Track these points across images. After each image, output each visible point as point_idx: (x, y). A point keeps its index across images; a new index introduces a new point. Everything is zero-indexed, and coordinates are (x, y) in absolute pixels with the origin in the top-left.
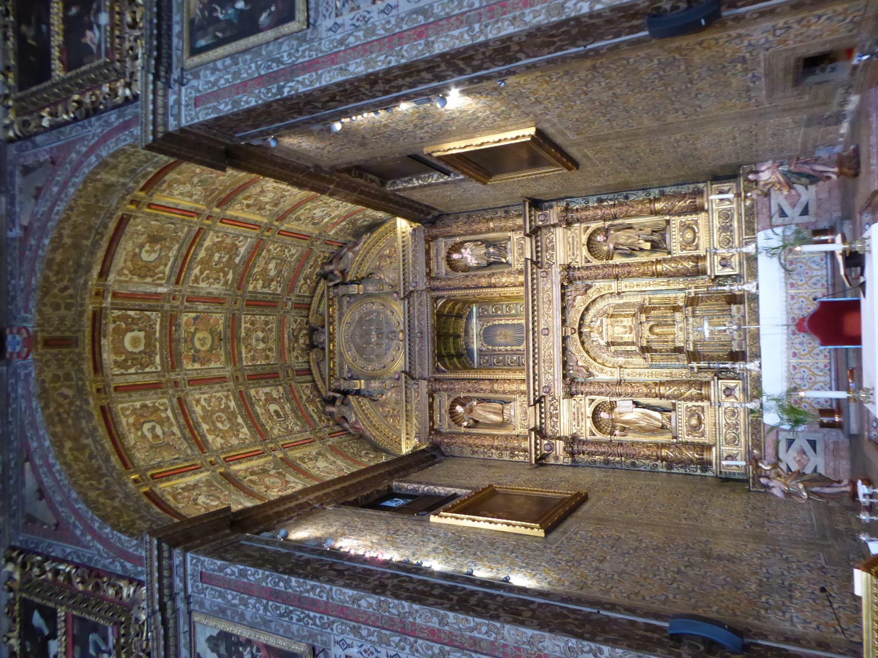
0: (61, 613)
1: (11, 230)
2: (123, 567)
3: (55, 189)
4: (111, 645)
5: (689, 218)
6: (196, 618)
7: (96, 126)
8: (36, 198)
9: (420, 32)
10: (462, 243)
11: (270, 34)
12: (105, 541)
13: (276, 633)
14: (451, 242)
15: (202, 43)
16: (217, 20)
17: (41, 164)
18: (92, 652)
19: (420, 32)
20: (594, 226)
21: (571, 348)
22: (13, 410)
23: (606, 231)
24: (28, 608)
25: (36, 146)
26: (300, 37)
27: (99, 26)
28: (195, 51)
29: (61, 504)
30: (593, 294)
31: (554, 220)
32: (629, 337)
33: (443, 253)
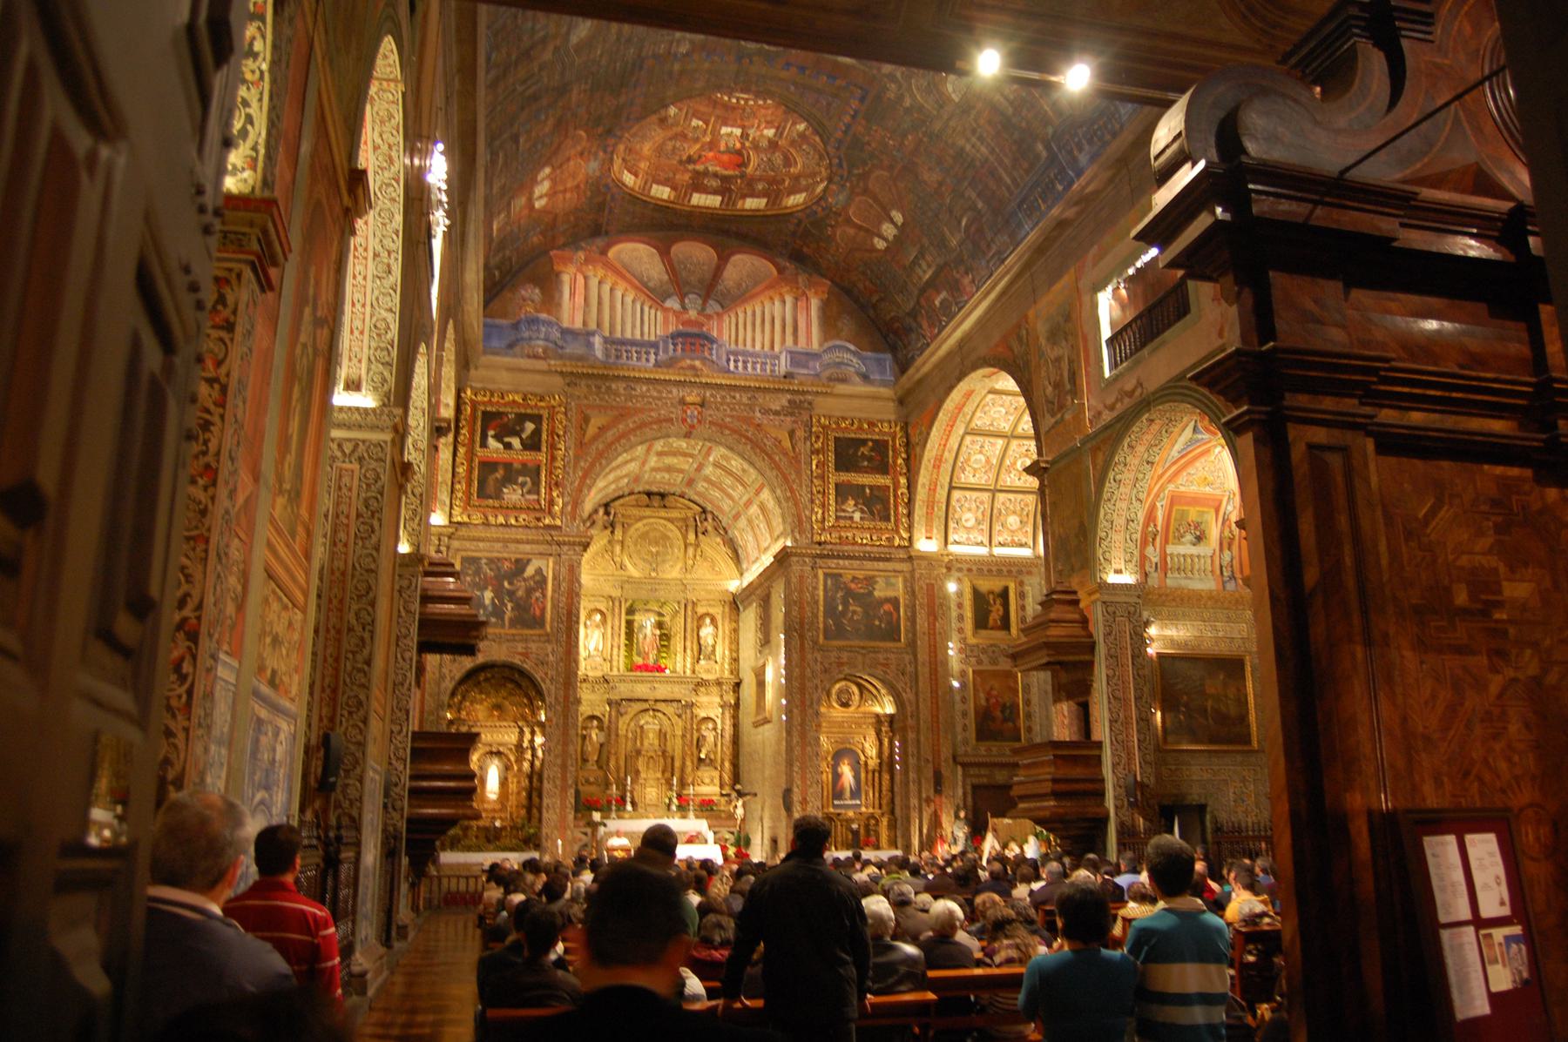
0: (542, 457)
4: (528, 497)
5: (717, 781)
6: (551, 560)
7: (805, 498)
9: (803, 702)
10: (716, 627)
11: (821, 626)
14: (719, 618)
15: (829, 582)
18: (521, 479)
19: (803, 702)
20: (719, 722)
21: (639, 704)
23: (715, 729)
24: (537, 419)
28: (826, 575)
30: (675, 719)
31: (725, 698)
32: (646, 743)
33: (711, 611)
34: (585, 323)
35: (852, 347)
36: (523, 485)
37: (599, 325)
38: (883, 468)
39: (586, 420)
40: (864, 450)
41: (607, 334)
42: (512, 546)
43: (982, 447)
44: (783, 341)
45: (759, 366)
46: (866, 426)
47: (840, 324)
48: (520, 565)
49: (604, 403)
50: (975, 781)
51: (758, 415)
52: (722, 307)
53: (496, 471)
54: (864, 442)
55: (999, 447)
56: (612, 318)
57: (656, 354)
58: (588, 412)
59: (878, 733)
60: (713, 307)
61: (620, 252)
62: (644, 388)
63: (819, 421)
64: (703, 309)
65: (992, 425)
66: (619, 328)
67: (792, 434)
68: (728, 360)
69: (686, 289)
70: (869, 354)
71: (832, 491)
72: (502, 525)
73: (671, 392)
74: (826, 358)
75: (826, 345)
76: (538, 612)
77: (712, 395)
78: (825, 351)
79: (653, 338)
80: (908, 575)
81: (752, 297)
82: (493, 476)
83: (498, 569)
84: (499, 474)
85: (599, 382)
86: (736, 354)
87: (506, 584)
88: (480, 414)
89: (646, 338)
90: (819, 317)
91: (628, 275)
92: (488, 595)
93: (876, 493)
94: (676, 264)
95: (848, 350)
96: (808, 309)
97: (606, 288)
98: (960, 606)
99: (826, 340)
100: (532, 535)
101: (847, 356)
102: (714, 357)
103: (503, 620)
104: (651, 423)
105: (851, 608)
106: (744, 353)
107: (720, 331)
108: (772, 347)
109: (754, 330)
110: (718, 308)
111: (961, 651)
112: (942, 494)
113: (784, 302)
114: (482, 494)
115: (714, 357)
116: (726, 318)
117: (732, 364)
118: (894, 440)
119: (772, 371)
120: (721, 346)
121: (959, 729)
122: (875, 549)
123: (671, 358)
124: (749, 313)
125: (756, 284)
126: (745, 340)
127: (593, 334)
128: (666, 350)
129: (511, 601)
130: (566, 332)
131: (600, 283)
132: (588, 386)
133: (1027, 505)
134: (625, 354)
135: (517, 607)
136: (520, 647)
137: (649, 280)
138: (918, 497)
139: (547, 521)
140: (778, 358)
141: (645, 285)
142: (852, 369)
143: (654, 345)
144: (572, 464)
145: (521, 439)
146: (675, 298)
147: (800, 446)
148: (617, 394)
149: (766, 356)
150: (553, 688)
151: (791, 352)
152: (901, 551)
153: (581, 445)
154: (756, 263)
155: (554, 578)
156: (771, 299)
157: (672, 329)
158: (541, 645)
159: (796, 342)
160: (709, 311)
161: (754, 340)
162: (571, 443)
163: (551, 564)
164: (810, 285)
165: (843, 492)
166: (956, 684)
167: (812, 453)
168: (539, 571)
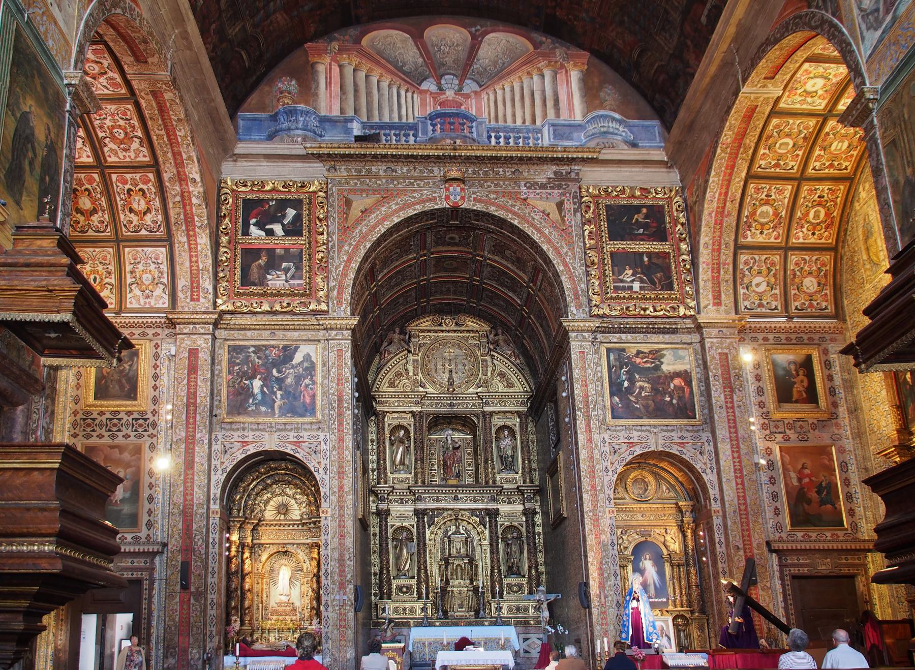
0: (302, 240)
1: (525, 185)
2: (334, 287)
3: (547, 232)
4: (292, 282)
7: (580, 270)
8: (543, 212)
12: (345, 274)
13: (322, 400)
16: (621, 369)
17: (563, 217)
18: (284, 265)
22: (412, 184)
24: (297, 204)
25: (576, 211)
26: (603, 422)
27: (632, 281)
29: (361, 231)
34: (342, 111)
35: (617, 116)
36: (287, 270)
37: (356, 111)
38: (661, 235)
39: (348, 203)
40: (639, 217)
41: (365, 120)
42: (280, 334)
43: (768, 196)
44: (545, 115)
45: (521, 140)
46: (638, 193)
47: (602, 94)
48: (288, 353)
49: (365, 187)
50: (794, 571)
51: (523, 189)
52: (480, 86)
53: (260, 258)
54: (638, 209)
55: (787, 194)
56: (369, 103)
57: (415, 136)
58: (351, 196)
59: (681, 528)
60: (470, 86)
61: (372, 40)
62: (405, 169)
63: (587, 191)
64: (461, 89)
65: (777, 165)
66: (376, 113)
67: (560, 206)
68: (489, 137)
69: (442, 70)
70: (636, 122)
71: (608, 261)
72: (268, 313)
73: (432, 171)
74: (591, 128)
75: (590, 116)
76: (308, 400)
77: (474, 172)
78: (588, 122)
79: (411, 120)
80: (698, 347)
81: (509, 74)
82: (257, 263)
83: (267, 357)
84: (262, 261)
85: (359, 165)
86: (497, 130)
87: (274, 372)
88: (240, 201)
89: (404, 120)
90: (580, 89)
91: (383, 61)
92: (257, 384)
93: (654, 260)
94: (430, 48)
95: (613, 119)
96: (568, 82)
97: (362, 75)
98: (758, 378)
99: (589, 111)
100: (297, 321)
101: (615, 125)
102: (475, 135)
103: (273, 408)
104: (414, 204)
105: (638, 384)
106: (506, 129)
107: (479, 109)
108: (534, 122)
109: (513, 106)
110: (475, 87)
111: (764, 427)
112: (727, 256)
113: (543, 76)
114: (245, 281)
115: (475, 135)
116: (484, 96)
117: (493, 141)
118: (670, 205)
119: (535, 144)
120: (481, 123)
121: (769, 513)
122: (659, 320)
123: (431, 138)
124: (508, 89)
125: (513, 60)
126: (505, 115)
127: (351, 120)
128: (425, 132)
129: (280, 389)
130: (324, 120)
131: (355, 70)
132: (348, 170)
133: (824, 265)
134: (384, 138)
135: (287, 395)
136: (291, 436)
137: (404, 64)
138: (701, 260)
139: (311, 308)
140: (540, 131)
141: (400, 69)
142: (619, 138)
143: (413, 127)
144: (336, 249)
145: (283, 225)
146: (431, 80)
147: (569, 217)
148: (377, 177)
149: (528, 131)
150: (327, 477)
151: (553, 125)
152: (688, 321)
153: (345, 230)
154: (511, 40)
155: (324, 365)
156: (529, 73)
157: (429, 110)
158: (313, 433)
159: (558, 115)
160: (466, 90)
161: (514, 115)
162: (334, 228)
163: (319, 351)
164: (568, 58)
165: (620, 260)
166: (763, 462)
167: (584, 224)
168: (307, 357)
